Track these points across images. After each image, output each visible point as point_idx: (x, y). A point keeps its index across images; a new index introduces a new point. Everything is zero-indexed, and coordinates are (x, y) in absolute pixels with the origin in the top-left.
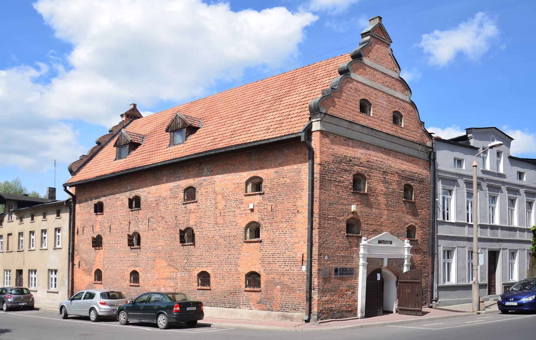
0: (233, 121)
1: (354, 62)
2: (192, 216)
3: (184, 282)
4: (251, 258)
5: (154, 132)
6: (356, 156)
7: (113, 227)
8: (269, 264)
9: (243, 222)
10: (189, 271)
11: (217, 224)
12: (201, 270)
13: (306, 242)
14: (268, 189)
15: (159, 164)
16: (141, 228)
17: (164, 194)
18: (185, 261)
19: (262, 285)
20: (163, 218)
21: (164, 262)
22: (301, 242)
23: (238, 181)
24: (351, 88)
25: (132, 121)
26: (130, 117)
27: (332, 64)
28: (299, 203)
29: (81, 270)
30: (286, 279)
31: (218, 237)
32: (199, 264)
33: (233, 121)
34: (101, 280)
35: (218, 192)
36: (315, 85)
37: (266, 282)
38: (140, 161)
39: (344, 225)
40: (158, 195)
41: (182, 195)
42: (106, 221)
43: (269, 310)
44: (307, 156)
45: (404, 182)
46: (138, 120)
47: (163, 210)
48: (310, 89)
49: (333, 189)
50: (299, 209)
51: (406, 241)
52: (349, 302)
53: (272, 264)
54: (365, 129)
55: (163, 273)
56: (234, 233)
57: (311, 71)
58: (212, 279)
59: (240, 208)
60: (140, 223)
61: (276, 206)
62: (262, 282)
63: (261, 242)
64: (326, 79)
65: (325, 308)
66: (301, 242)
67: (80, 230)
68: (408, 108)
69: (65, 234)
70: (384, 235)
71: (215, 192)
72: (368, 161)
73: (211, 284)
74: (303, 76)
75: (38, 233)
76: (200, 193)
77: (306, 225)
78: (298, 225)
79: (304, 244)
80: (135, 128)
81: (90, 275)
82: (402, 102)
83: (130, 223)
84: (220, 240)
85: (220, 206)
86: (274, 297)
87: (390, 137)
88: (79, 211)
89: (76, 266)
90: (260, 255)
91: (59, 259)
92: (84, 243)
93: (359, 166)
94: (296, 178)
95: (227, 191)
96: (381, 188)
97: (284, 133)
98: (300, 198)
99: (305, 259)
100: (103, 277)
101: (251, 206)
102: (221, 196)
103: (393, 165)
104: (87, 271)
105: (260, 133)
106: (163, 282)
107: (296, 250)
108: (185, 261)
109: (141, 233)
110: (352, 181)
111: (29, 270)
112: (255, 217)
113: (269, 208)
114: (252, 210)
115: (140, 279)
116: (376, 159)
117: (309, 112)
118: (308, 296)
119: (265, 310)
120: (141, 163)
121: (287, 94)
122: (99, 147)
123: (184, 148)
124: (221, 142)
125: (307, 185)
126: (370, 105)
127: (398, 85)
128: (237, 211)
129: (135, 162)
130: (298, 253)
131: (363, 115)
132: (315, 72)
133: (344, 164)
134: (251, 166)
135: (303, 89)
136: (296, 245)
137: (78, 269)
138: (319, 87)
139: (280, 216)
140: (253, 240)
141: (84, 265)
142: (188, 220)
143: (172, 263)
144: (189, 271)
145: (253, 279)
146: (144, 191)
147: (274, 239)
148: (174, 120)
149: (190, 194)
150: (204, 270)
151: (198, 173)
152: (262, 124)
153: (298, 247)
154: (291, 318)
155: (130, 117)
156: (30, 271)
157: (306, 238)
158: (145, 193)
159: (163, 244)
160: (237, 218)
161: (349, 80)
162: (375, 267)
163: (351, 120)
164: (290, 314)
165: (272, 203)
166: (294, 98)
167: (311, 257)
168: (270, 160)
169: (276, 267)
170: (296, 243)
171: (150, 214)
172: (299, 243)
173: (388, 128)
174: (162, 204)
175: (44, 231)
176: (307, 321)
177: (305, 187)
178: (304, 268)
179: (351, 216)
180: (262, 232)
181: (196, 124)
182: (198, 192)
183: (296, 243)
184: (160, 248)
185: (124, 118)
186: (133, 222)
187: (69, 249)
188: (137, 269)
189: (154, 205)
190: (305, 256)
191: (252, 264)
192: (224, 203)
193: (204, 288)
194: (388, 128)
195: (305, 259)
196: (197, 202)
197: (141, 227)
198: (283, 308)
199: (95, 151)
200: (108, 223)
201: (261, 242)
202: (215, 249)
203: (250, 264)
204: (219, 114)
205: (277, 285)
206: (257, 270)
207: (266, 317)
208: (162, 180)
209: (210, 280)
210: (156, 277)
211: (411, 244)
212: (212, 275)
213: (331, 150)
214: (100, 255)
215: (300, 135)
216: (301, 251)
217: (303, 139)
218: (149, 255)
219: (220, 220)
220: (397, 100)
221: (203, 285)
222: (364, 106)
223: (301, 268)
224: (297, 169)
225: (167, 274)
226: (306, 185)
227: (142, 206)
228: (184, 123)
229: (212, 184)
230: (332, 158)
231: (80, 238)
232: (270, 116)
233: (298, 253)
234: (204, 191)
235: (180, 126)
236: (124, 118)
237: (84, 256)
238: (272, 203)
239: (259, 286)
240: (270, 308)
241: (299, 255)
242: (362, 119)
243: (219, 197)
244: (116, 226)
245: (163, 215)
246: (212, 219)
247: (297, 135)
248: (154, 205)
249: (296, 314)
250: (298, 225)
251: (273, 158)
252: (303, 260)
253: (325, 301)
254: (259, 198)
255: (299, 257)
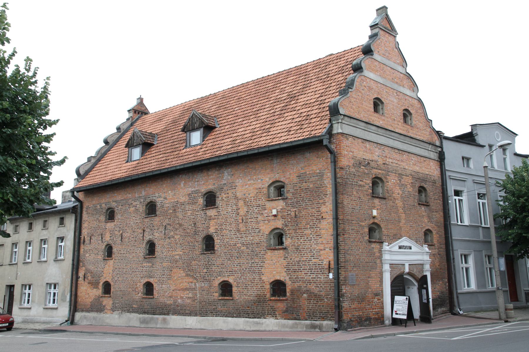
0: (250, 121)
1: (366, 58)
2: (212, 223)
3: (204, 293)
4: (274, 267)
5: (167, 130)
6: (373, 159)
7: (125, 235)
8: (295, 272)
9: (266, 229)
10: (209, 281)
11: (239, 231)
12: (222, 280)
13: (332, 249)
14: (291, 194)
15: (178, 168)
16: (157, 236)
17: (183, 199)
18: (205, 270)
19: (288, 294)
20: (181, 225)
21: (182, 272)
22: (327, 249)
23: (260, 186)
24: (365, 87)
25: (139, 117)
26: (137, 112)
27: (343, 59)
28: (323, 209)
29: (86, 283)
30: (312, 287)
31: (240, 245)
32: (220, 274)
33: (250, 121)
34: (110, 294)
35: (240, 197)
36: (329, 82)
37: (292, 291)
38: (155, 164)
39: (367, 230)
40: (176, 200)
41: (201, 201)
42: (118, 229)
43: (295, 319)
44: (329, 160)
45: (417, 185)
46: (146, 116)
47: (181, 216)
48: (324, 87)
49: (355, 193)
50: (323, 215)
51: (424, 245)
52: (376, 309)
53: (298, 272)
54: (380, 130)
55: (180, 284)
56: (257, 240)
57: (322, 65)
58: (234, 289)
59: (262, 214)
60: (155, 231)
61: (300, 212)
62: (288, 290)
63: (285, 249)
64: (340, 75)
65: (353, 316)
66: (327, 249)
67: (87, 239)
68: (416, 105)
69: (69, 244)
70: (405, 241)
71: (236, 198)
72: (384, 164)
73: (233, 294)
74: (315, 71)
75: (36, 244)
76: (220, 198)
77: (331, 231)
78: (323, 232)
79: (330, 251)
80: (145, 126)
81: (97, 288)
82: (410, 100)
83: (144, 231)
84: (242, 248)
85: (242, 212)
86: (300, 306)
87: (402, 137)
88: (86, 219)
89: (81, 279)
90: (285, 263)
91: (59, 272)
92: (92, 254)
93: (377, 169)
94: (318, 182)
95: (249, 196)
96: (397, 192)
97: (306, 135)
98: (324, 203)
99: (332, 266)
100: (112, 290)
101: (274, 212)
102: (243, 202)
103: (407, 167)
104: (94, 284)
105: (281, 135)
106: (181, 294)
107: (322, 258)
108: (205, 270)
109: (156, 241)
110: (371, 185)
111: (23, 285)
112: (279, 224)
113: (293, 214)
114: (275, 216)
115: (154, 291)
116: (391, 160)
117: (328, 113)
118: (337, 304)
119: (292, 319)
120: (158, 166)
121: (302, 91)
122: (107, 147)
123: (203, 150)
124: (241, 144)
125: (331, 190)
126: (382, 103)
127: (406, 82)
128: (260, 218)
129: (151, 165)
130: (325, 260)
131: (376, 115)
132: (327, 67)
133: (363, 168)
134: (272, 170)
135: (317, 86)
136: (322, 252)
137: (83, 282)
138: (333, 84)
139: (304, 222)
140: (277, 247)
141: (89, 278)
142: (208, 227)
143: (190, 272)
144: (209, 281)
145: (278, 288)
146: (160, 197)
147: (299, 246)
148: (192, 119)
149: (210, 199)
150: (226, 279)
151: (218, 177)
152: (281, 126)
153: (324, 254)
154: (320, 328)
155: (137, 112)
156: (24, 286)
157: (332, 244)
158: (162, 199)
159: (181, 253)
160: (260, 225)
161: (363, 77)
162: (397, 273)
163: (367, 120)
164: (318, 323)
165: (296, 209)
166: (310, 97)
167: (338, 264)
168: (292, 164)
169: (302, 275)
170: (322, 250)
171: (167, 221)
172: (324, 250)
173: (400, 127)
174: (180, 210)
175: (44, 241)
176: (336, 330)
177: (328, 193)
178: (331, 276)
179: (372, 221)
180: (286, 239)
181: (211, 124)
182: (218, 197)
183: (322, 250)
184: (178, 257)
185: (131, 114)
186: (147, 230)
187: (73, 260)
188: (151, 280)
189: (171, 211)
190: (332, 262)
191: (277, 273)
192: (245, 209)
193: (226, 298)
194: (400, 127)
195: (332, 266)
196: (217, 207)
197: (156, 234)
198: (311, 316)
199: (103, 151)
200: (119, 231)
201: (285, 249)
202: (238, 258)
203: (274, 272)
204: (234, 112)
205: (304, 293)
206: (282, 279)
207: (292, 327)
208: (180, 184)
209: (232, 290)
210: (173, 288)
211: (429, 249)
212: (234, 284)
213: (351, 153)
214: (109, 266)
215: (322, 138)
216: (327, 258)
217: (325, 143)
218: (165, 264)
219: (242, 227)
220: (407, 97)
221: (225, 296)
222: (377, 104)
223: (328, 276)
224: (320, 173)
225: (185, 285)
226: (330, 190)
227: (157, 213)
228: (202, 122)
229: (232, 189)
230: (352, 162)
231: (86, 248)
232: (289, 115)
233: (325, 260)
234: (225, 196)
235: (196, 125)
236: (131, 114)
237: (91, 267)
238: (296, 209)
239: (285, 295)
240: (297, 317)
241: (325, 262)
242: (376, 119)
243: (241, 203)
244: (129, 234)
245: (181, 222)
246: (233, 225)
247: (319, 138)
248: (171, 211)
249: (325, 323)
250: (323, 232)
251: (295, 162)
252: (329, 267)
253: (354, 308)
254: (281, 204)
255: (325, 265)
